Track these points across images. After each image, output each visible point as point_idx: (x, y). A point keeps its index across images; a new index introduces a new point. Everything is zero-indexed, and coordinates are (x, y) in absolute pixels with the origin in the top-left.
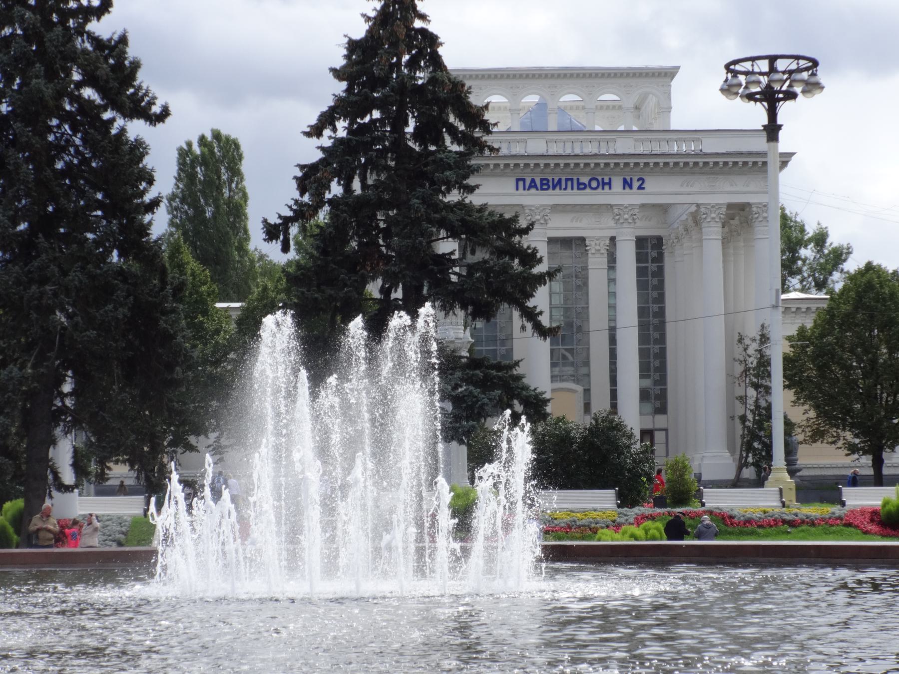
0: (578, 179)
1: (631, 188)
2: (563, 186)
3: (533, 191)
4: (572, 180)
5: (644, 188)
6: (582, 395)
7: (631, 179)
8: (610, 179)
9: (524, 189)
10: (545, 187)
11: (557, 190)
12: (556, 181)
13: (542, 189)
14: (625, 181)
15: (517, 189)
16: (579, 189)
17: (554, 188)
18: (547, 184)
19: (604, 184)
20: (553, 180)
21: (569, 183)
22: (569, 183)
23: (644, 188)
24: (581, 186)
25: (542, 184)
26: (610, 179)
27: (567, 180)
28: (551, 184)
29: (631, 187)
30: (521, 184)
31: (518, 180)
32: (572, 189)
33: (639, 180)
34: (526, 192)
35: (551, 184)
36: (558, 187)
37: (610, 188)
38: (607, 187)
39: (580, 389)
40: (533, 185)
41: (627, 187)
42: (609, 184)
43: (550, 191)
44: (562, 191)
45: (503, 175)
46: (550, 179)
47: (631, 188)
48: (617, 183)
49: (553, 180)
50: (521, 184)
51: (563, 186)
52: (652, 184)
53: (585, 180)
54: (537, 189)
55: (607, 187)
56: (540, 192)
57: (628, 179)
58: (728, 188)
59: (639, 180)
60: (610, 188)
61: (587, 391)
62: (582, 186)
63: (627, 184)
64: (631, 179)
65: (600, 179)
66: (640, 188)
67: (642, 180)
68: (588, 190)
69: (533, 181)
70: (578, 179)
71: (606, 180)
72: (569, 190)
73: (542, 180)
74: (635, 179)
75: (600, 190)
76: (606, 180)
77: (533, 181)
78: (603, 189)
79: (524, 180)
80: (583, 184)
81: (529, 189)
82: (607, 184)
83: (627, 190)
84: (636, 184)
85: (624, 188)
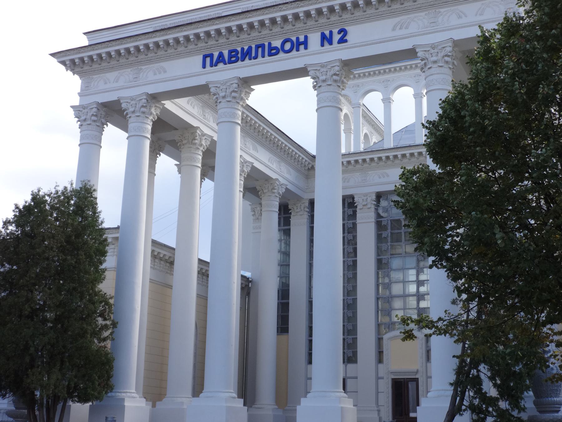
0: (270, 44)
1: (331, 43)
2: (253, 55)
3: (221, 65)
4: (263, 46)
5: (346, 41)
7: (331, 33)
8: (306, 37)
9: (211, 66)
10: (233, 59)
11: (247, 61)
13: (230, 62)
15: (204, 66)
16: (270, 55)
17: (243, 60)
19: (299, 44)
20: (243, 49)
21: (260, 50)
22: (260, 50)
23: (346, 41)
24: (273, 51)
25: (230, 57)
26: (306, 37)
27: (258, 47)
28: (239, 55)
30: (208, 60)
31: (205, 57)
32: (263, 56)
34: (214, 68)
35: (239, 55)
36: (247, 57)
37: (306, 48)
38: (302, 47)
41: (326, 43)
42: (305, 43)
43: (240, 63)
44: (253, 61)
45: (190, 54)
46: (239, 49)
47: (331, 43)
48: (314, 39)
49: (243, 49)
50: (208, 60)
51: (253, 55)
52: (355, 33)
53: (277, 43)
55: (302, 47)
56: (228, 65)
57: (327, 33)
59: (339, 32)
60: (306, 48)
62: (274, 51)
63: (326, 39)
64: (331, 33)
65: (294, 39)
66: (342, 41)
67: (343, 32)
68: (281, 55)
69: (221, 55)
70: (270, 44)
71: (302, 39)
72: (260, 59)
73: (230, 52)
74: (335, 31)
75: (294, 52)
76: (302, 39)
77: (221, 55)
78: (298, 50)
79: (211, 56)
80: (276, 48)
81: (216, 65)
82: (302, 43)
84: (336, 37)
85: (322, 45)
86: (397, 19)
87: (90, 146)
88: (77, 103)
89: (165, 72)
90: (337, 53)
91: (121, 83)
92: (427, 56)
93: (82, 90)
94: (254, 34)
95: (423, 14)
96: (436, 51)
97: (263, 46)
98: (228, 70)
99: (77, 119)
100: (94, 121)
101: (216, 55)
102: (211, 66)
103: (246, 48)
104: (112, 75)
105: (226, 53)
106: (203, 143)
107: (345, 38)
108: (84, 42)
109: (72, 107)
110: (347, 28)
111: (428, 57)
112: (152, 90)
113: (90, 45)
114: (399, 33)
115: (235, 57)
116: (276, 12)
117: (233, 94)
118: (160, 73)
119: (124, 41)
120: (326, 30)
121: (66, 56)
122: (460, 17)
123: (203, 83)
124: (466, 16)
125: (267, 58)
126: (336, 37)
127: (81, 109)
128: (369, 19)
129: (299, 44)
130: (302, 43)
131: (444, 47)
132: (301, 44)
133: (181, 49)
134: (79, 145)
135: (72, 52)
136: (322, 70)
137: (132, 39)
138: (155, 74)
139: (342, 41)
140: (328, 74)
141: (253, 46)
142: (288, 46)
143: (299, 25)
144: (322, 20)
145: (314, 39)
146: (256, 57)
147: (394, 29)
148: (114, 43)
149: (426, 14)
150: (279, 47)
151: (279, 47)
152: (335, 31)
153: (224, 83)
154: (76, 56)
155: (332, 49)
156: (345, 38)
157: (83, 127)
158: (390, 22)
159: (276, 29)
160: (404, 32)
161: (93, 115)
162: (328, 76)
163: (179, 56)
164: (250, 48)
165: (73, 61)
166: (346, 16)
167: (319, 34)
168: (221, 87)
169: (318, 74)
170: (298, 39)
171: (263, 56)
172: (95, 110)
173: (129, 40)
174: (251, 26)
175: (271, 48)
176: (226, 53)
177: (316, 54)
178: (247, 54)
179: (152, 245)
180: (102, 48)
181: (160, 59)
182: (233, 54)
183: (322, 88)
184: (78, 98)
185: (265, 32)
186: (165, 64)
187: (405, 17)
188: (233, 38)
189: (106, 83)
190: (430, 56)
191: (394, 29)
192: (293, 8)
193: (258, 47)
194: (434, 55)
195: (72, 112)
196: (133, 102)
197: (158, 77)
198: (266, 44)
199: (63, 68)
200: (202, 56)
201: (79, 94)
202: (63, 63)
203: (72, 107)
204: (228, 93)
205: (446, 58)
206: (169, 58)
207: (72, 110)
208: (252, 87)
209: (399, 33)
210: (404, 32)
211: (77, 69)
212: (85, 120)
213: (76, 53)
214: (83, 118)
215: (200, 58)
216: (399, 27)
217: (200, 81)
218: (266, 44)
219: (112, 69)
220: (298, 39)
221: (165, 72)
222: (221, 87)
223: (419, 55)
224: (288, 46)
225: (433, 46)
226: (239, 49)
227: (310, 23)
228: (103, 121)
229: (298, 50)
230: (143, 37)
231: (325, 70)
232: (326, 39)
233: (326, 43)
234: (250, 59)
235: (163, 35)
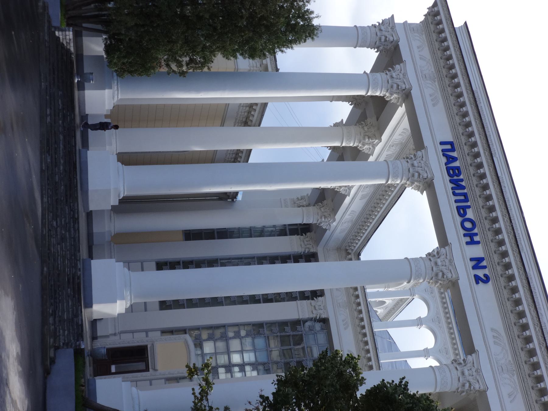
0: (469, 207)
1: (474, 268)
2: (457, 191)
3: (444, 160)
4: (466, 200)
5: (477, 283)
7: (485, 267)
8: (478, 243)
9: (443, 150)
10: (451, 172)
11: (450, 186)
13: (448, 169)
14: (482, 259)
15: (442, 143)
16: (458, 208)
17: (451, 181)
19: (471, 236)
20: (462, 180)
21: (462, 198)
22: (462, 198)
23: (477, 283)
24: (462, 211)
25: (453, 168)
26: (478, 243)
27: (465, 195)
28: (455, 178)
30: (449, 147)
31: (451, 144)
32: (456, 201)
34: (441, 153)
35: (455, 178)
36: (454, 186)
37: (467, 243)
38: (468, 239)
40: (451, 159)
41: (474, 263)
42: (472, 242)
43: (448, 178)
44: (451, 191)
45: (453, 128)
46: (461, 177)
47: (474, 268)
48: (477, 251)
49: (462, 180)
50: (449, 147)
51: (457, 191)
52: (486, 291)
53: (470, 214)
54: (446, 164)
55: (468, 239)
56: (445, 167)
57: (484, 263)
58: (505, 390)
59: (485, 275)
60: (467, 243)
62: (462, 211)
63: (477, 263)
64: (485, 267)
65: (476, 231)
66: (478, 279)
67: (487, 280)
68: (459, 219)
69: (454, 159)
71: (476, 239)
72: (453, 198)
73: (458, 168)
74: (486, 271)
75: (462, 232)
76: (476, 239)
77: (454, 159)
78: (465, 235)
79: (453, 150)
80: (465, 213)
81: (444, 155)
82: (472, 239)
84: (480, 273)
85: (472, 259)
87: (355, 37)
88: (397, 21)
89: (434, 105)
90: (464, 275)
92: (468, 365)
93: (410, 24)
94: (478, 191)
95: (510, 358)
96: (474, 374)
97: (466, 200)
98: (440, 168)
99: (381, 22)
100: (380, 39)
101: (454, 154)
102: (443, 151)
103: (463, 184)
104: (426, 53)
105: (456, 164)
106: (366, 146)
107: (480, 282)
108: (458, 23)
109: (393, 16)
110: (490, 282)
111: (467, 366)
112: (415, 93)
113: (454, 28)
114: (489, 335)
115: (454, 173)
116: (501, 211)
117: (416, 174)
118: (432, 100)
119: (461, 63)
120: (487, 263)
121: (443, 6)
122: (510, 395)
123: (426, 144)
124: (511, 402)
125: (455, 205)
126: (480, 273)
127: (391, 25)
128: (501, 304)
129: (471, 236)
130: (472, 239)
131: (478, 381)
132: (471, 239)
133: (458, 119)
134: (355, 26)
135: (447, 13)
136: (447, 261)
137: (464, 71)
138: (431, 95)
139: (478, 279)
140: (443, 267)
141: (465, 191)
142: (468, 225)
143: (490, 235)
144: (496, 258)
145: (477, 251)
146: (454, 194)
147: (492, 330)
148: (458, 53)
149: (510, 361)
150: (467, 217)
151: (467, 217)
153: (427, 165)
154: (442, 16)
155: (468, 269)
156: (480, 282)
157: (374, 29)
158: (499, 325)
159: (484, 213)
160: (491, 341)
161: (386, 37)
162: (441, 267)
163: (451, 118)
164: (463, 188)
165: (438, 14)
166: (502, 281)
167: (483, 256)
168: (422, 162)
169: (443, 257)
170: (476, 234)
171: (456, 201)
172: (391, 39)
173: (463, 67)
174: (486, 187)
175: (465, 208)
176: (456, 164)
177: (462, 254)
178: (457, 185)
179: (262, 104)
180: (452, 41)
181: (446, 99)
182: (457, 171)
184: (402, 22)
185: (481, 202)
186: (441, 105)
188: (472, 170)
189: (418, 47)
190: (469, 368)
191: (492, 330)
192: (506, 228)
193: (465, 195)
194: (470, 372)
195: (387, 16)
196: (401, 76)
198: (469, 204)
200: (452, 140)
201: (406, 22)
203: (393, 16)
204: (417, 169)
205: (467, 385)
206: (448, 109)
207: (390, 16)
208: (425, 192)
209: (489, 335)
210: (491, 341)
211: (430, 18)
212: (381, 30)
213: (445, 17)
214: (382, 28)
215: (450, 139)
216: (495, 335)
217: (427, 141)
218: (469, 204)
219: (433, 53)
220: (476, 234)
221: (434, 105)
223: (469, 357)
224: (468, 225)
225: (479, 371)
226: (461, 177)
227: (493, 246)
228: (381, 48)
229: (465, 235)
230: (467, 81)
232: (477, 263)
233: (474, 263)
234: (452, 188)
235: (469, 100)
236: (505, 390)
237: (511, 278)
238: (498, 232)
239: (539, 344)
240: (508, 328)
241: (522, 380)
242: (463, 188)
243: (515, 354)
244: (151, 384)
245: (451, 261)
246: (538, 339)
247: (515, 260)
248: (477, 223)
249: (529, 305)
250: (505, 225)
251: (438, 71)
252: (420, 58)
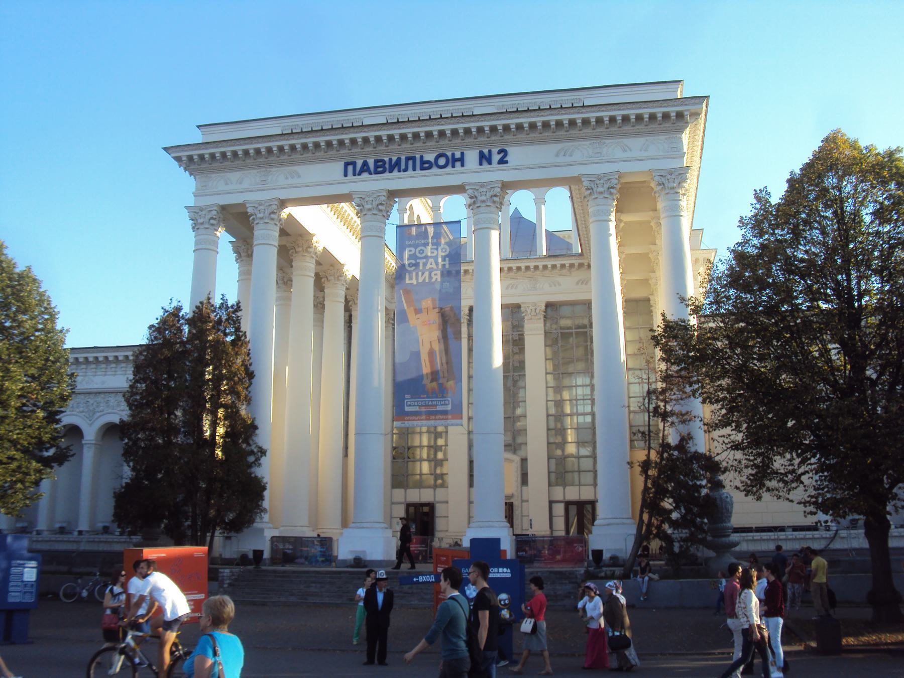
0: (422, 157)
1: (490, 163)
2: (403, 167)
3: (365, 175)
5: (506, 162)
6: (519, 464)
7: (490, 151)
8: (462, 154)
10: (380, 169)
11: (395, 173)
12: (393, 161)
13: (376, 173)
15: (346, 175)
16: (422, 169)
17: (391, 171)
18: (383, 166)
19: (455, 160)
20: (390, 160)
21: (411, 163)
22: (411, 163)
23: (506, 162)
24: (426, 165)
25: (376, 167)
26: (462, 154)
27: (408, 159)
28: (387, 166)
29: (490, 162)
30: (350, 168)
31: (347, 164)
33: (499, 152)
34: (357, 177)
35: (387, 166)
36: (396, 169)
37: (463, 165)
38: (458, 164)
39: (516, 459)
40: (365, 168)
41: (484, 162)
42: (462, 160)
43: (387, 174)
44: (402, 173)
45: (329, 160)
46: (387, 159)
47: (490, 163)
48: (472, 157)
49: (390, 160)
50: (350, 168)
51: (403, 167)
52: (515, 154)
53: (430, 157)
54: (370, 174)
55: (458, 164)
57: (486, 151)
58: (619, 154)
59: (499, 152)
60: (463, 165)
61: (524, 461)
62: (427, 165)
63: (485, 158)
64: (490, 151)
65: (449, 154)
66: (502, 161)
67: (503, 152)
68: (435, 170)
69: (365, 164)
70: (422, 157)
71: (458, 155)
73: (376, 162)
74: (495, 151)
75: (449, 169)
76: (458, 155)
77: (365, 164)
78: (453, 167)
79: (354, 164)
81: (359, 174)
82: (458, 160)
83: (486, 166)
84: (496, 158)
85: (481, 164)
86: (559, 146)
87: (205, 251)
89: (299, 176)
90: (494, 174)
91: (246, 185)
93: (197, 189)
94: (406, 146)
95: (588, 143)
96: (602, 182)
101: (359, 163)
102: (354, 175)
103: (394, 159)
104: (234, 176)
105: (371, 162)
108: (197, 137)
112: (283, 195)
114: (561, 159)
115: (380, 167)
116: (433, 125)
117: (380, 207)
118: (293, 177)
122: (625, 151)
125: (419, 172)
126: (496, 158)
128: (531, 142)
129: (455, 160)
130: (458, 160)
135: (191, 148)
136: (481, 190)
137: (265, 139)
138: (287, 178)
139: (502, 161)
141: (403, 158)
142: (442, 161)
143: (457, 141)
144: (482, 139)
145: (472, 157)
146: (406, 170)
147: (557, 155)
148: (242, 142)
152: (495, 151)
154: (195, 153)
158: (554, 147)
159: (432, 143)
160: (568, 159)
161: (212, 218)
163: (316, 160)
164: (399, 160)
165: (190, 158)
170: (453, 154)
171: (414, 170)
173: (260, 140)
174: (403, 137)
175: (423, 162)
176: (371, 162)
177: (472, 171)
178: (395, 166)
180: (227, 146)
181: (293, 163)
183: (481, 209)
185: (419, 144)
186: (299, 169)
187: (571, 144)
188: (381, 148)
189: (227, 184)
191: (557, 155)
192: (453, 124)
193: (408, 159)
194: (600, 185)
195: (186, 214)
197: (291, 181)
198: (418, 156)
199: (176, 163)
200: (343, 163)
202: (178, 159)
206: (304, 162)
209: (561, 159)
210: (568, 159)
215: (340, 165)
216: (562, 153)
217: (344, 189)
218: (418, 156)
219: (237, 168)
220: (453, 154)
221: (299, 176)
222: (367, 199)
224: (442, 161)
229: (453, 167)
231: (484, 190)
232: (485, 158)
233: (484, 162)
234: (399, 171)
236: (619, 154)
237: (506, 128)
238: (455, 132)
239: (578, 113)
240: (557, 140)
241: (610, 136)
242: (399, 160)
243: (584, 138)
244: (527, 501)
245: (482, 185)
246: (573, 113)
247: (488, 121)
248: (441, 152)
249: (538, 116)
250: (449, 124)
251: (259, 166)
252: (241, 183)
